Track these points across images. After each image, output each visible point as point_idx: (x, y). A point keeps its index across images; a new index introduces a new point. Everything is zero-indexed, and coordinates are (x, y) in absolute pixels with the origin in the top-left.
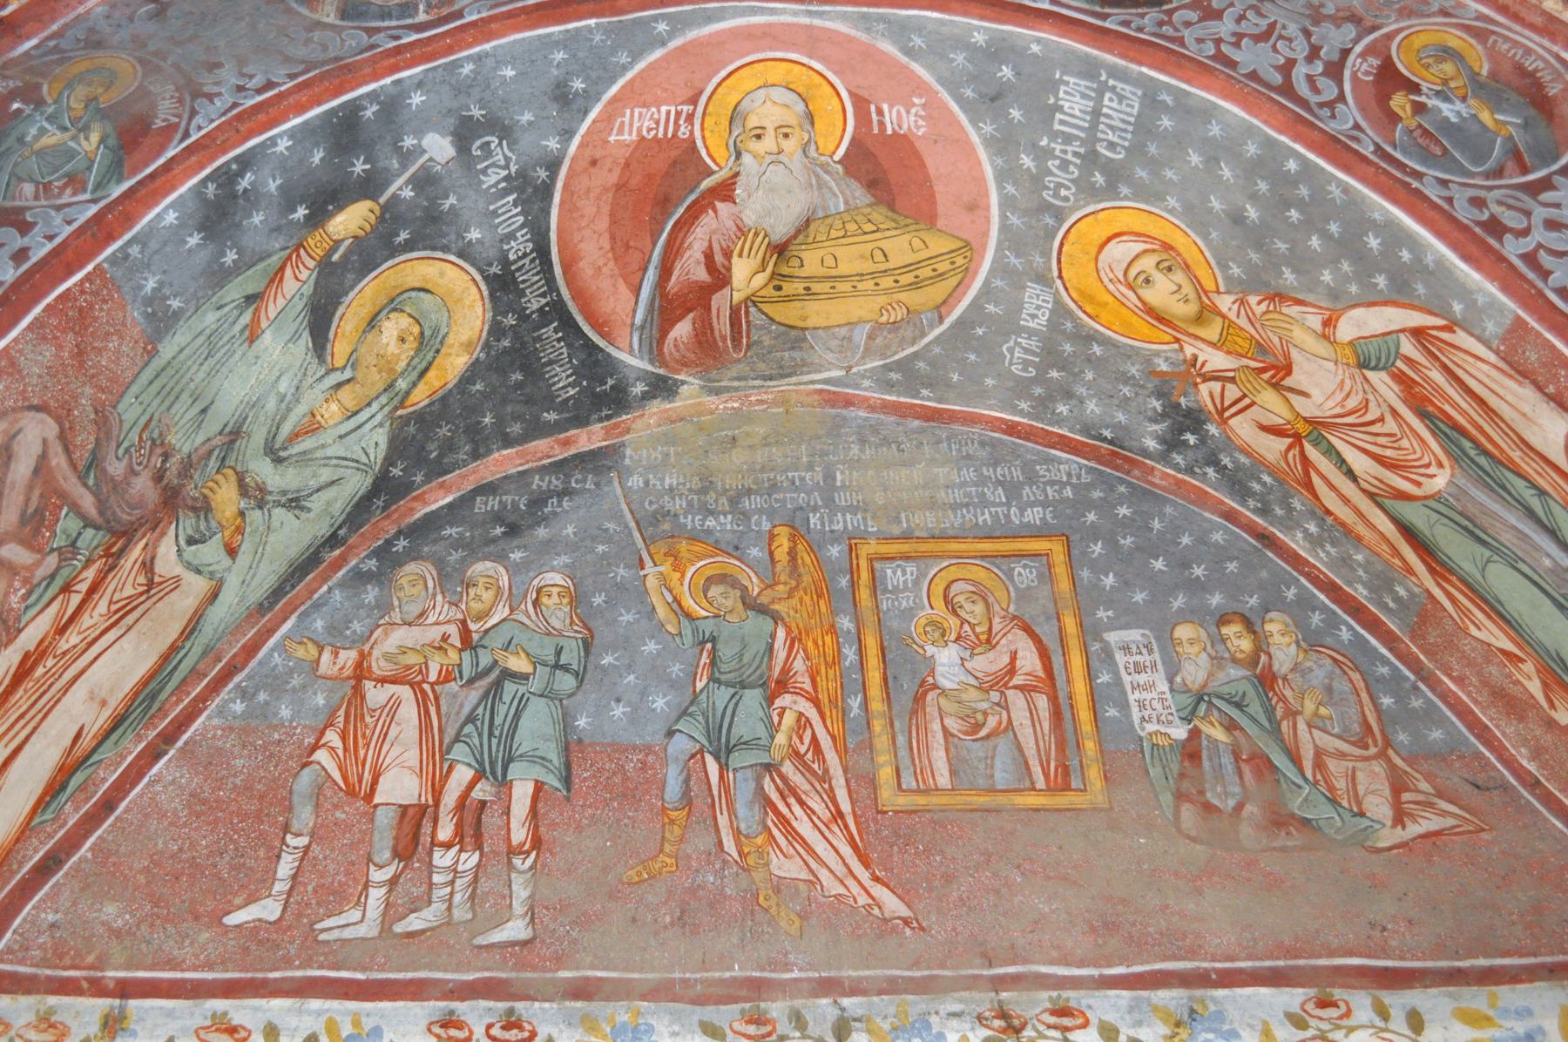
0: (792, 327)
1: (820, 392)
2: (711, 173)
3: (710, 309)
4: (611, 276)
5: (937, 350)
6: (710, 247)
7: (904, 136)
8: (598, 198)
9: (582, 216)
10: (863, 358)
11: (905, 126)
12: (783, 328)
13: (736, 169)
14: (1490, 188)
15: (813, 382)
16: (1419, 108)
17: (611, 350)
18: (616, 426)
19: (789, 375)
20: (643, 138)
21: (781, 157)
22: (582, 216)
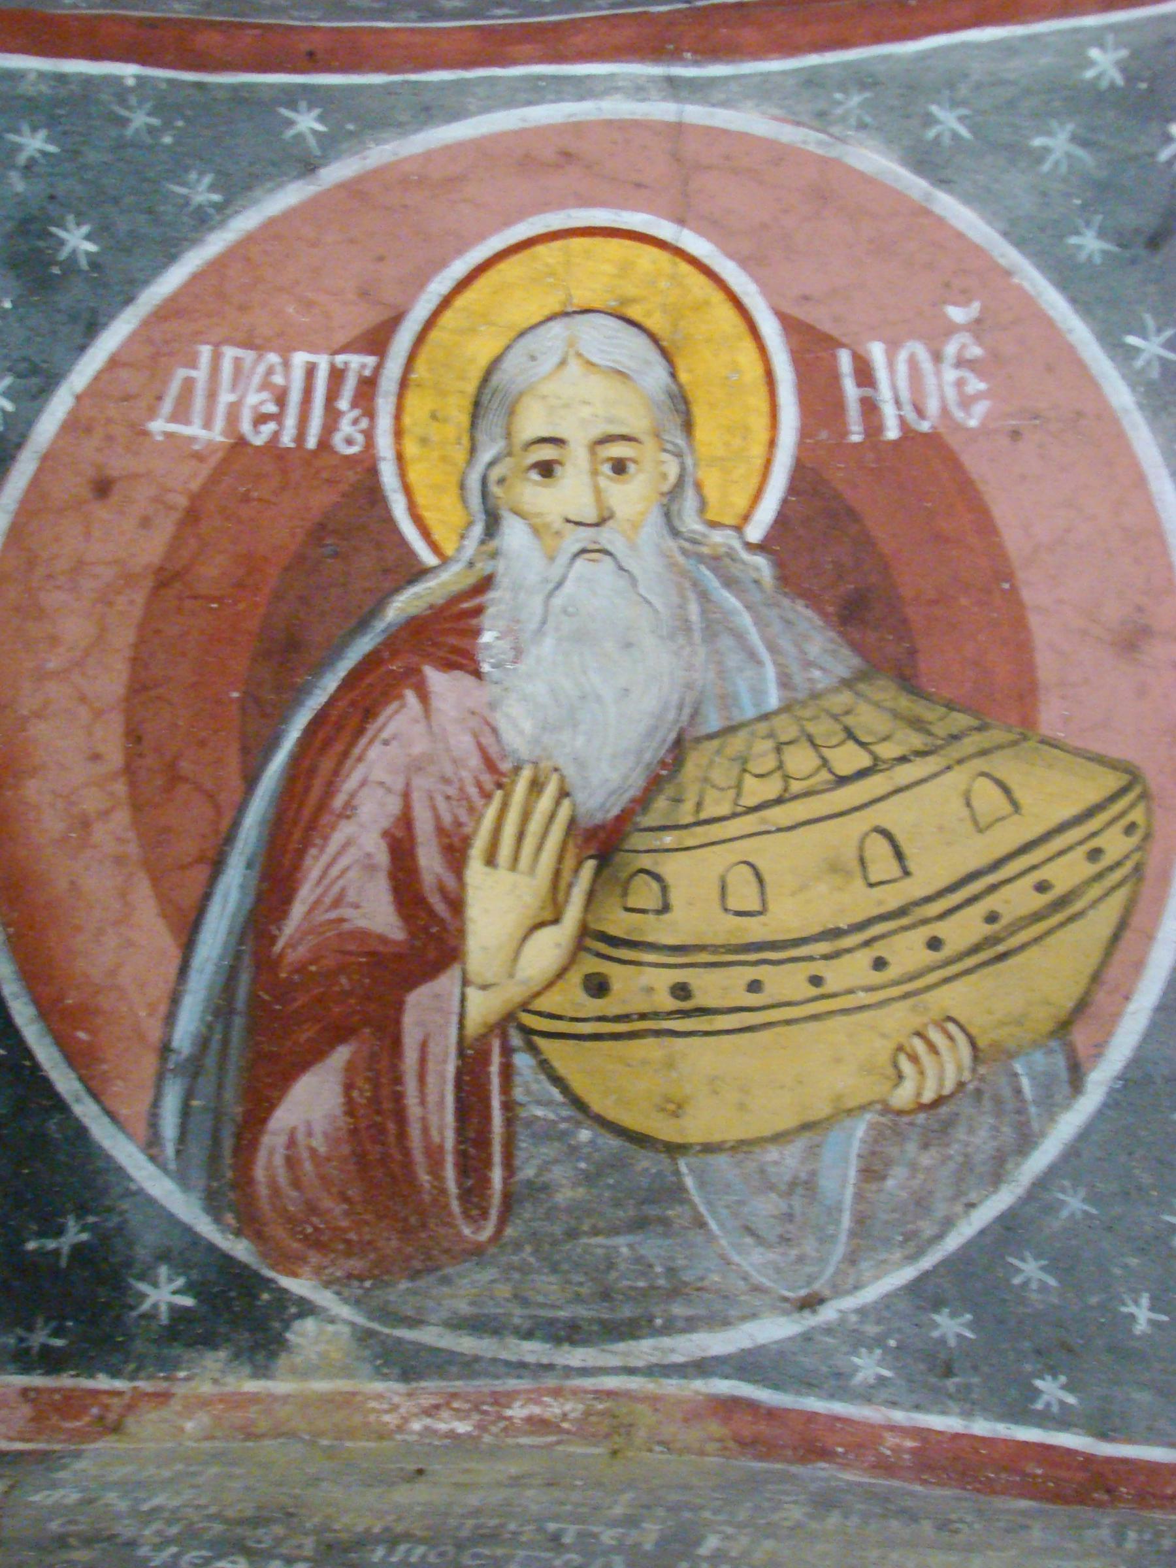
0: (640, 1140)
1: (729, 1406)
2: (420, 573)
3: (396, 1044)
4: (119, 860)
5: (1074, 1203)
6: (406, 820)
7: (932, 440)
8: (105, 599)
9: (54, 641)
10: (852, 1259)
11: (932, 406)
12: (613, 1143)
13: (484, 567)
15: (702, 1367)
17: (86, 1111)
18: (71, 1404)
19: (629, 1330)
20: (241, 443)
21: (607, 537)
22: (54, 641)
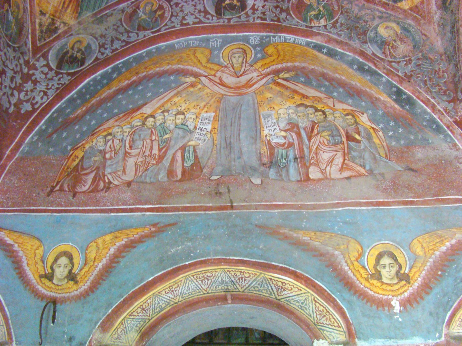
14: (4, 38)
16: (7, 11)
